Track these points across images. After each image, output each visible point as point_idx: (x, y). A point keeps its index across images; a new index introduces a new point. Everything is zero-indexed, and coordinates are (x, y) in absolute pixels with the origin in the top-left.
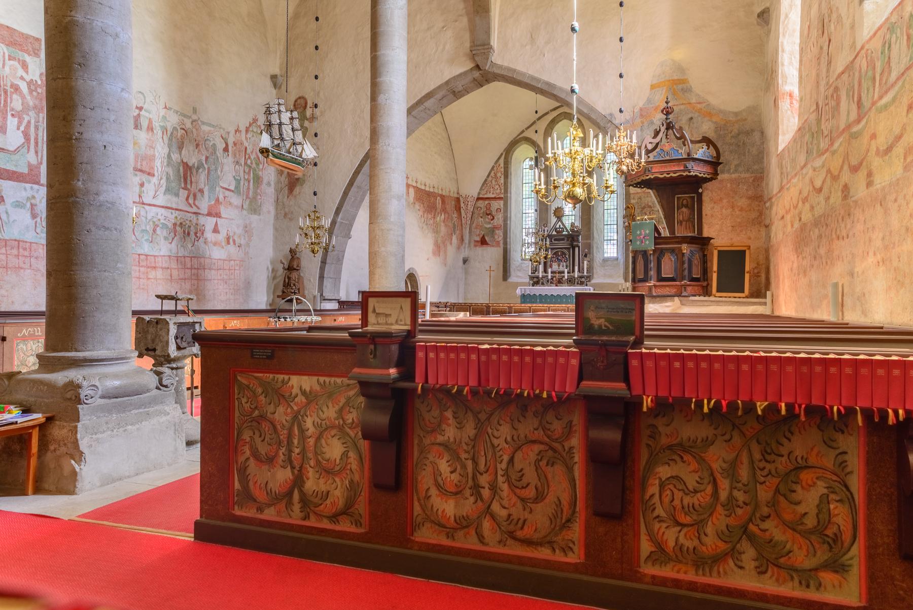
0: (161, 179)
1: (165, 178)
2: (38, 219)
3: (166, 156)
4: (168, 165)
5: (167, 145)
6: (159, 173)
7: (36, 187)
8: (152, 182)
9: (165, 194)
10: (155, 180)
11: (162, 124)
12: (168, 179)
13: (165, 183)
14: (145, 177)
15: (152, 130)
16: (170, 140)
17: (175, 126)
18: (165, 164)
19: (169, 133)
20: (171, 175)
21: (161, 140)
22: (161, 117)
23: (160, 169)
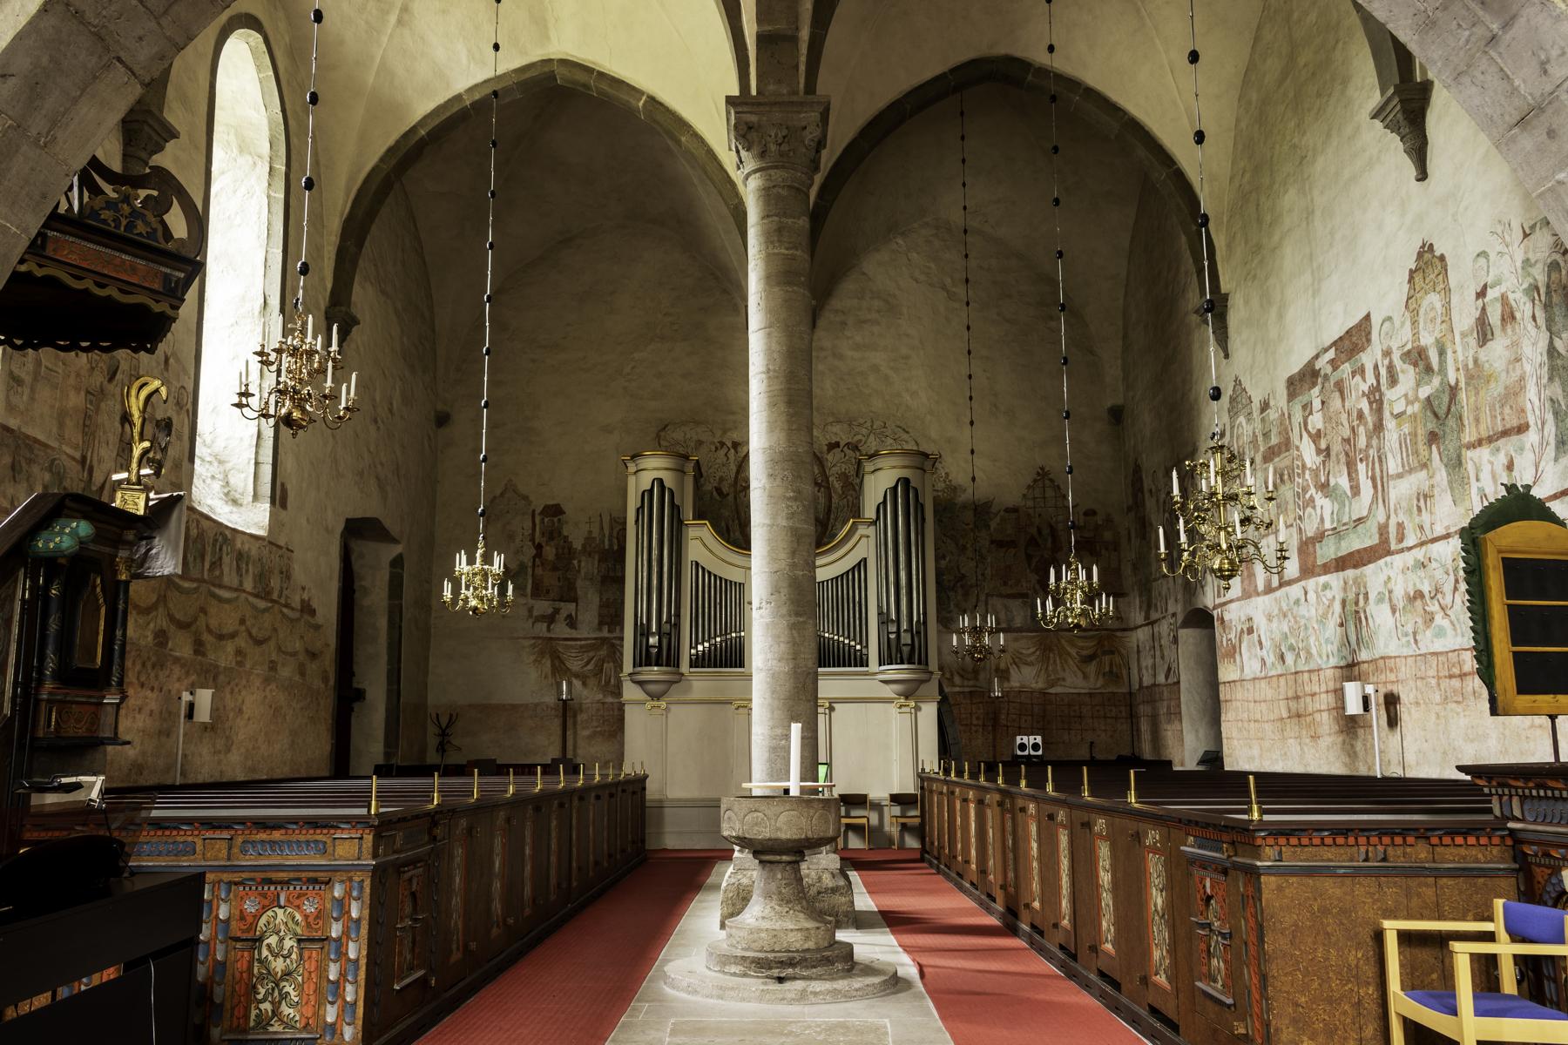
0: (1543, 424)
1: (1550, 417)
2: (1397, 614)
3: (1545, 358)
4: (1551, 379)
5: (1544, 328)
6: (1537, 412)
7: (1388, 559)
8: (1528, 446)
9: (1556, 460)
10: (1532, 437)
11: (1525, 285)
12: (1556, 414)
13: (1554, 429)
14: (1508, 445)
15: (1514, 318)
16: (1547, 307)
17: (1549, 261)
18: (1545, 380)
19: (1543, 290)
20: (1561, 398)
21: (1530, 326)
22: (1520, 271)
23: (1537, 403)
